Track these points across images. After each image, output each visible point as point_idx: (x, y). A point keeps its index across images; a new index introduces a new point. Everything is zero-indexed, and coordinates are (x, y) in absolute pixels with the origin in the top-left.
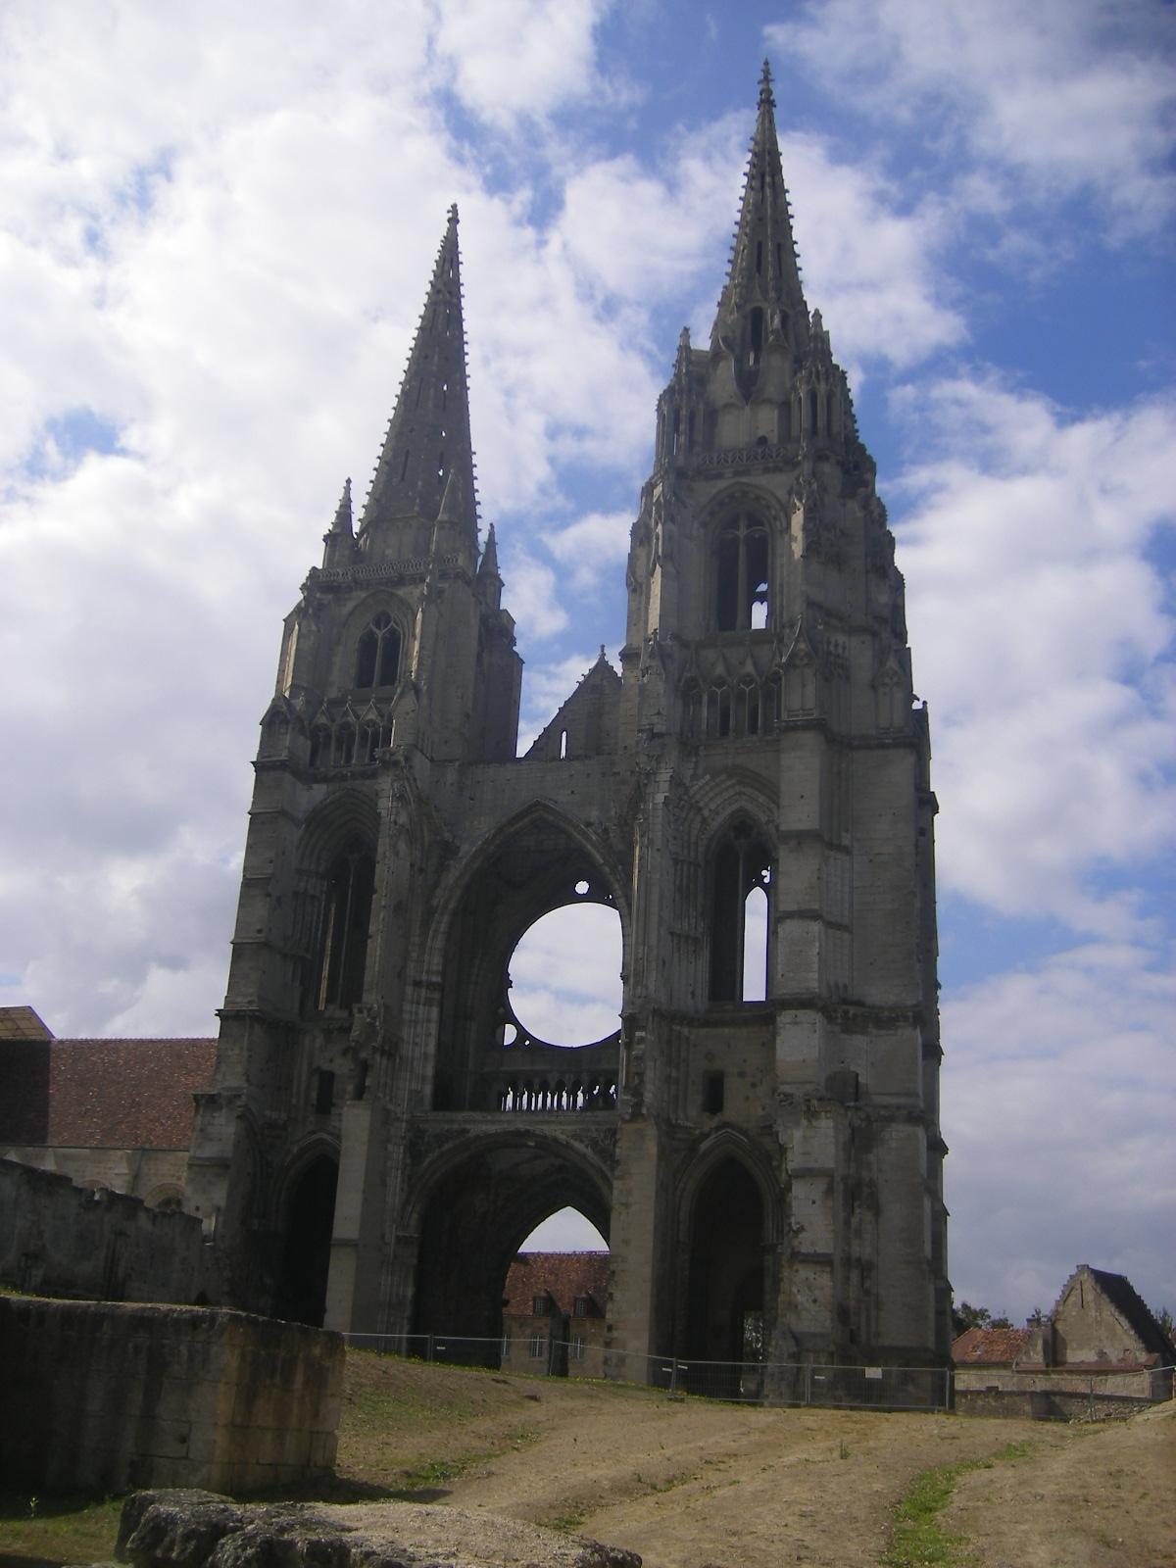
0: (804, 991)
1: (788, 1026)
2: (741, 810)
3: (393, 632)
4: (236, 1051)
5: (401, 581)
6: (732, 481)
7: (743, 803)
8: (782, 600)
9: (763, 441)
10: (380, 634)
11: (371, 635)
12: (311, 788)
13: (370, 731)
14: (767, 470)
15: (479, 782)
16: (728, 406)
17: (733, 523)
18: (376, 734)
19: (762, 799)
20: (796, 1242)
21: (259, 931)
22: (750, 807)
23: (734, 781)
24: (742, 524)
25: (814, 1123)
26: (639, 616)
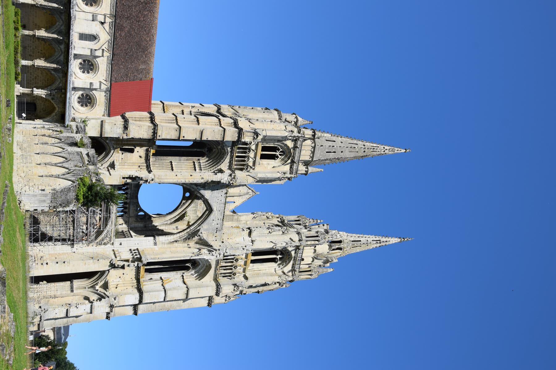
0: (145, 299)
1: (135, 297)
2: (200, 264)
3: (278, 157)
4: (143, 133)
6: (293, 256)
7: (201, 265)
8: (256, 271)
9: (303, 260)
13: (246, 159)
14: (293, 264)
16: (315, 251)
17: (282, 254)
19: (201, 271)
20: (73, 307)
21: (184, 137)
22: (200, 267)
23: (208, 265)
24: (280, 256)
25: (108, 307)
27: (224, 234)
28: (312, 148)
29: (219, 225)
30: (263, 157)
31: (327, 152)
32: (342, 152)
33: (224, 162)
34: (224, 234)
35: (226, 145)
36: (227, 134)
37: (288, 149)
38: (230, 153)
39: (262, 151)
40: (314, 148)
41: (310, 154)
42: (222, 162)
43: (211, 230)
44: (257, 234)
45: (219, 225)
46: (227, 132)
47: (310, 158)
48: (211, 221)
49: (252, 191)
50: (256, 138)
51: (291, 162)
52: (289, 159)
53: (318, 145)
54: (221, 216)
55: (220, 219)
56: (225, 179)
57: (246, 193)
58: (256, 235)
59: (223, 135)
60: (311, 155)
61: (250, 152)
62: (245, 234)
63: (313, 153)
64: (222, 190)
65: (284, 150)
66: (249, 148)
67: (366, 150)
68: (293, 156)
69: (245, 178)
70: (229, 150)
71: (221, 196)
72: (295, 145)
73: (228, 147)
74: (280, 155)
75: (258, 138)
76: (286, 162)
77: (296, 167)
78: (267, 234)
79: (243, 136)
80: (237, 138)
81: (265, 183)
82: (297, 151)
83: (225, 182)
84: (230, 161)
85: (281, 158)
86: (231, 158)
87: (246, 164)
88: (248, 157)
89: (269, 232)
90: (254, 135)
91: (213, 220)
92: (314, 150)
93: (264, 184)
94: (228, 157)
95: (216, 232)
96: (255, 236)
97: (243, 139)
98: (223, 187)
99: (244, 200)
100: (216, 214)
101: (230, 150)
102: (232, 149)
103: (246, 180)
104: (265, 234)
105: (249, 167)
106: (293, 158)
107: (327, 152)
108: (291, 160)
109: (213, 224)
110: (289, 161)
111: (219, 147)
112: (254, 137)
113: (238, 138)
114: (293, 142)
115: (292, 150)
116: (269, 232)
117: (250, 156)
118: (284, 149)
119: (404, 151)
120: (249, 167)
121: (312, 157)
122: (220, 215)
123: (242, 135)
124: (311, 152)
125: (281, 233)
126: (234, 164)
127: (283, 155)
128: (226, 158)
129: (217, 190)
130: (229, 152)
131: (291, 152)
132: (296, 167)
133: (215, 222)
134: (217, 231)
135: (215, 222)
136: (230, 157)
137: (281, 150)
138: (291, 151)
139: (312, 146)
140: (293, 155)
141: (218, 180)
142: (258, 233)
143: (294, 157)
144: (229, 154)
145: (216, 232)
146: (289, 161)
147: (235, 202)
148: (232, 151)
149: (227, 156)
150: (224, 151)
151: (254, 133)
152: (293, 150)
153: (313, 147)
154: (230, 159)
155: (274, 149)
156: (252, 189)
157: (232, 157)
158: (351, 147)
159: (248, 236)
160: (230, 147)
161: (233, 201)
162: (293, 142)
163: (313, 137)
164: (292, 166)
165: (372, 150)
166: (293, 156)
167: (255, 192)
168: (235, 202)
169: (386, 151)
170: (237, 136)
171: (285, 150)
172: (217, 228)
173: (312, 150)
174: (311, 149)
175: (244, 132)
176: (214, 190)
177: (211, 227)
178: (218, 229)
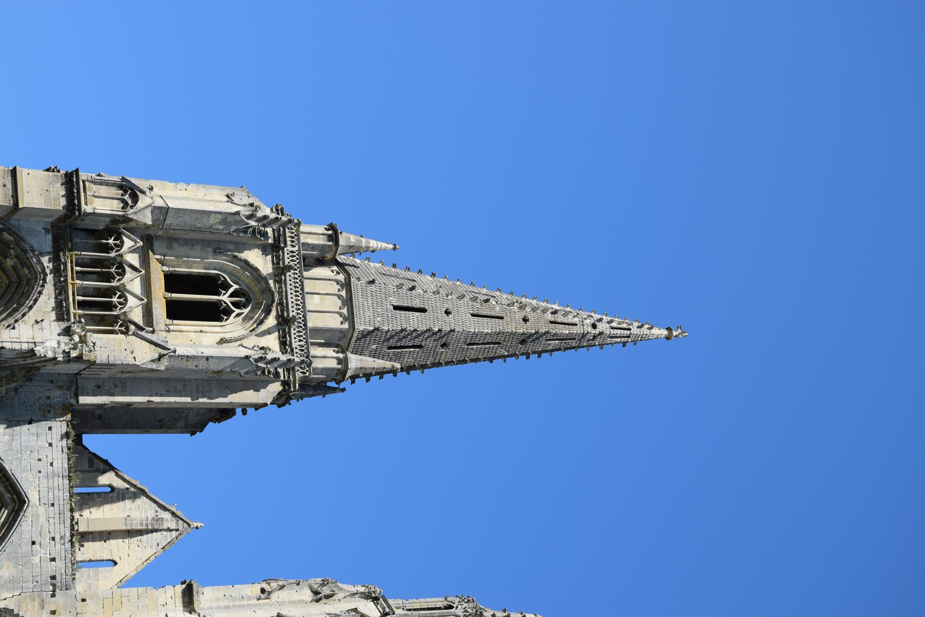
3: (228, 312)
5: (284, 322)
10: (225, 298)
11: (226, 287)
12: (47, 231)
13: (115, 299)
15: (50, 428)
18: (110, 306)
26: (235, 599)
27: (84, 600)
28: (339, 287)
29: (59, 564)
30: (176, 311)
31: (396, 308)
32: (447, 313)
33: (35, 308)
34: (84, 600)
35: (32, 247)
36: (24, 186)
37: (256, 279)
38: (55, 277)
39: (168, 289)
40: (347, 285)
41: (340, 308)
42: (31, 308)
43: (31, 585)
44: (217, 600)
45: (59, 564)
46: (24, 179)
47: (342, 323)
48: (26, 548)
49: (173, 514)
50: (130, 202)
51: (279, 324)
52: (268, 312)
53: (359, 279)
54: (62, 526)
55: (62, 538)
56: (48, 344)
57: (150, 518)
58: (215, 605)
59: (9, 186)
60: (345, 311)
61: (123, 273)
62: (169, 601)
63: (348, 302)
64: (49, 424)
65: (244, 288)
66: (119, 259)
67: (531, 316)
68: (281, 304)
69: (124, 346)
70: (46, 265)
71: (50, 445)
72: (276, 264)
73: (42, 254)
74: (233, 303)
75: (139, 202)
76: (261, 322)
77: (302, 343)
78: (255, 601)
79: (82, 194)
80: (63, 202)
81: (204, 397)
82: (288, 283)
83: (50, 355)
84: (56, 302)
85: (238, 315)
86: (60, 294)
87: (117, 317)
88: (123, 292)
89: (263, 591)
90: (122, 195)
91: (33, 543)
92: (349, 291)
93: (201, 400)
94: (49, 289)
95: (53, 596)
96: (211, 608)
97: (86, 204)
98: (49, 412)
99: (149, 552)
100: (43, 519)
101: (51, 265)
102: (56, 259)
103: (129, 353)
104: (249, 598)
105: (132, 327)
106: (282, 311)
107: (396, 308)
108: (278, 317)
109: (36, 560)
110: (271, 321)
111: (9, 262)
112: (123, 201)
113: (68, 200)
114: (269, 257)
115: (271, 282)
116: (263, 591)
117: (128, 287)
118: (246, 285)
119: (665, 332)
120: (132, 327)
121: (350, 318)
122: (57, 521)
123: (79, 193)
124: (339, 303)
125: (307, 595)
126: (75, 315)
127: (245, 306)
128: (40, 293)
129: (30, 423)
130: (48, 271)
131: (270, 289)
132: (302, 343)
133: (41, 553)
134: (54, 591)
135: (41, 553)
136: (55, 290)
137: (235, 287)
138: (267, 284)
139: (338, 282)
140: (281, 299)
141: (25, 347)
142: (221, 595)
143: (283, 306)
144: (50, 278)
145: (53, 596)
146: (271, 321)
147: (115, 563)
148: (59, 265)
149: (43, 286)
150: (30, 272)
151: (120, 187)
152: (275, 282)
153: (342, 286)
154: (56, 298)
155: (211, 284)
156: (173, 509)
157: (61, 289)
158: (474, 299)
159: (182, 608)
160: (48, 253)
161: (106, 556)
162: (269, 257)
163: (331, 243)
164: (285, 337)
165: (549, 316)
166: (281, 304)
167: (183, 518)
168: (115, 563)
169: (599, 325)
170: (64, 193)
171: (249, 288)
172: (53, 578)
173: (343, 293)
174: (339, 290)
175: (84, 182)
176: (18, 423)
177: (27, 573)
178: (58, 577)
